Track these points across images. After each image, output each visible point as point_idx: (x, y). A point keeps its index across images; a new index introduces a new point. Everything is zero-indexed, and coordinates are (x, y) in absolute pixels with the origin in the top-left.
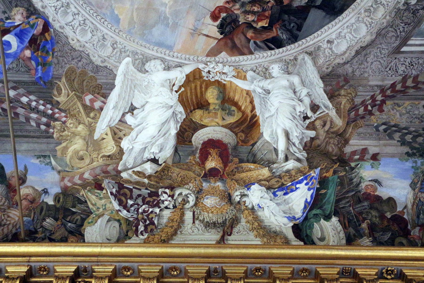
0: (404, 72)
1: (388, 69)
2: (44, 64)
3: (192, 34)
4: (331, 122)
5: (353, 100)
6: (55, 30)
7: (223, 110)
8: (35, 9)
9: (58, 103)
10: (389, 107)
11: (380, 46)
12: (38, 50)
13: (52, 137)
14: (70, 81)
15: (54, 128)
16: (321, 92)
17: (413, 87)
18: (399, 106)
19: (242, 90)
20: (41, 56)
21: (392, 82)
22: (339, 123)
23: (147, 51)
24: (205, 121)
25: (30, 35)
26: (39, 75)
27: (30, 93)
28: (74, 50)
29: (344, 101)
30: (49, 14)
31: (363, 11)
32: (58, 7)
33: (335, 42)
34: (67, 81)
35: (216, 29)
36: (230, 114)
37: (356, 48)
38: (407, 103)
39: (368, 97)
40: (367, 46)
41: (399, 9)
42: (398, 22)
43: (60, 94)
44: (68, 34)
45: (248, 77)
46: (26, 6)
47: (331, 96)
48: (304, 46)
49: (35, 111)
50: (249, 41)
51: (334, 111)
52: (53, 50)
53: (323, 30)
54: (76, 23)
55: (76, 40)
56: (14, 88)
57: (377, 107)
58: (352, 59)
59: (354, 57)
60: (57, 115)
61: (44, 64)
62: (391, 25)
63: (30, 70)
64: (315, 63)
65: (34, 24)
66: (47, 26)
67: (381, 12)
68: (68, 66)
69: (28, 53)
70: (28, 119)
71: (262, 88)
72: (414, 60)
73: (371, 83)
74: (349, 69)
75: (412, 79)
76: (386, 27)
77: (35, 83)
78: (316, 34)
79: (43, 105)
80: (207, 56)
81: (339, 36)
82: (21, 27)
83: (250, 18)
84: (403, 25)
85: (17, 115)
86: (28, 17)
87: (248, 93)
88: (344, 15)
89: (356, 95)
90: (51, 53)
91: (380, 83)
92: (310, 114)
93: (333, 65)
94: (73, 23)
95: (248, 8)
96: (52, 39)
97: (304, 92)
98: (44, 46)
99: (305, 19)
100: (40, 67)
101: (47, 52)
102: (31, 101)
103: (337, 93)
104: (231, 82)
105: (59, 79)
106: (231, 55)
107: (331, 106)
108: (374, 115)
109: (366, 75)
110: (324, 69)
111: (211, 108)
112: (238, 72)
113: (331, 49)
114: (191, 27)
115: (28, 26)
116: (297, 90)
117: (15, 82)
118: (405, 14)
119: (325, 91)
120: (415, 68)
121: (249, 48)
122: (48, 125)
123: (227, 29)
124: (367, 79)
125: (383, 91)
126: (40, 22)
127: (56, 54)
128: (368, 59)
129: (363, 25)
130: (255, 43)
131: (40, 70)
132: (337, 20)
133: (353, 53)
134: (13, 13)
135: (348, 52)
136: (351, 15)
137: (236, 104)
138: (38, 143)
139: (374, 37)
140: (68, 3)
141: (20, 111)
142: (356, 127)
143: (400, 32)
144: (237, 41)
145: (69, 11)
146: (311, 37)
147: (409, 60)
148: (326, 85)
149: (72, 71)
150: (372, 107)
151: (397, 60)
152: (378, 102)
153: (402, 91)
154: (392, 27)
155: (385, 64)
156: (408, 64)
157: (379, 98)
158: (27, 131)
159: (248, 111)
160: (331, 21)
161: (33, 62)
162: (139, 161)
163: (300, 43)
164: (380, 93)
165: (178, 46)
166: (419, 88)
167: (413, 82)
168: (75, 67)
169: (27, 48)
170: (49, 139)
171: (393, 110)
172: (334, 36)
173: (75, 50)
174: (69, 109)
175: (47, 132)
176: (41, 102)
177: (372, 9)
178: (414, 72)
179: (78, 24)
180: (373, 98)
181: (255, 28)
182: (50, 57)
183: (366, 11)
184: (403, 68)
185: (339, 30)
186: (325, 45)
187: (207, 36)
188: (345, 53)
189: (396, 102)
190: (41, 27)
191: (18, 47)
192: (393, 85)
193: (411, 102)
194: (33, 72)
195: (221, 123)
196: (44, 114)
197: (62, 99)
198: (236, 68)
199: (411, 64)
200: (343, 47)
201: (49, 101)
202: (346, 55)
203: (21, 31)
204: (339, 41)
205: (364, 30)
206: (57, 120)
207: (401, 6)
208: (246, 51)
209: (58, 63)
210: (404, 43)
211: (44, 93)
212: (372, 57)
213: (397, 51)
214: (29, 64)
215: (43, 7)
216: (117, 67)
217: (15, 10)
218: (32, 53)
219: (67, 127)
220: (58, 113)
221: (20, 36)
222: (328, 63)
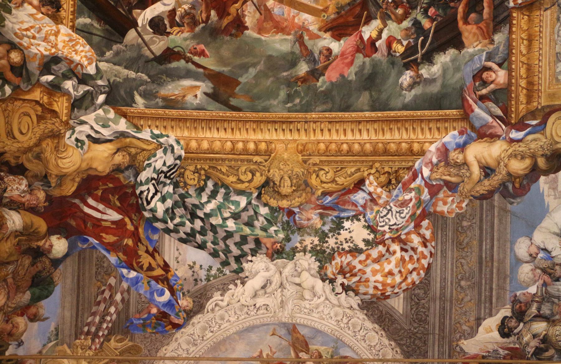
2: (144, 326)
6: (174, 334)
8: (191, 317)
9: (109, 340)
12: (156, 320)
13: (76, 338)
15: (85, 339)
20: (151, 322)
25: (170, 313)
26: (135, 322)
27: (118, 313)
30: (187, 329)
32: (193, 337)
34: (128, 347)
43: (117, 341)
44: (171, 345)
46: (194, 309)
49: (102, 320)
52: (157, 333)
55: (165, 352)
56: (123, 300)
60: (97, 340)
61: (144, 326)
63: (140, 313)
65: (179, 316)
66: (178, 327)
68: (143, 347)
69: (154, 311)
70: (94, 314)
77: (127, 319)
79: (107, 327)
82: (176, 305)
85: (99, 304)
86: (185, 311)
90: (154, 331)
94: (180, 349)
96: (166, 331)
98: (160, 325)
100: (142, 322)
101: (155, 328)
102: (111, 315)
105: (131, 340)
115: (177, 310)
117: (128, 301)
126: (180, 321)
127: (153, 335)
131: (138, 322)
134: (188, 298)
138: (71, 326)
140: (196, 345)
145: (191, 345)
158: (83, 314)
161: (146, 316)
168: (142, 353)
169: (159, 310)
170: (74, 336)
173: (157, 352)
174: (103, 351)
175: (81, 333)
176: (110, 325)
179: (180, 353)
182: (151, 331)
190: (177, 322)
191: (159, 302)
194: (138, 316)
196: (99, 328)
197: (113, 343)
201: (111, 332)
203: (173, 305)
206: (93, 340)
209: (145, 338)
211: (119, 326)
214: (144, 312)
215: (193, 323)
217: (190, 300)
218: (154, 315)
219: (86, 351)
220: (99, 341)
221: (169, 304)
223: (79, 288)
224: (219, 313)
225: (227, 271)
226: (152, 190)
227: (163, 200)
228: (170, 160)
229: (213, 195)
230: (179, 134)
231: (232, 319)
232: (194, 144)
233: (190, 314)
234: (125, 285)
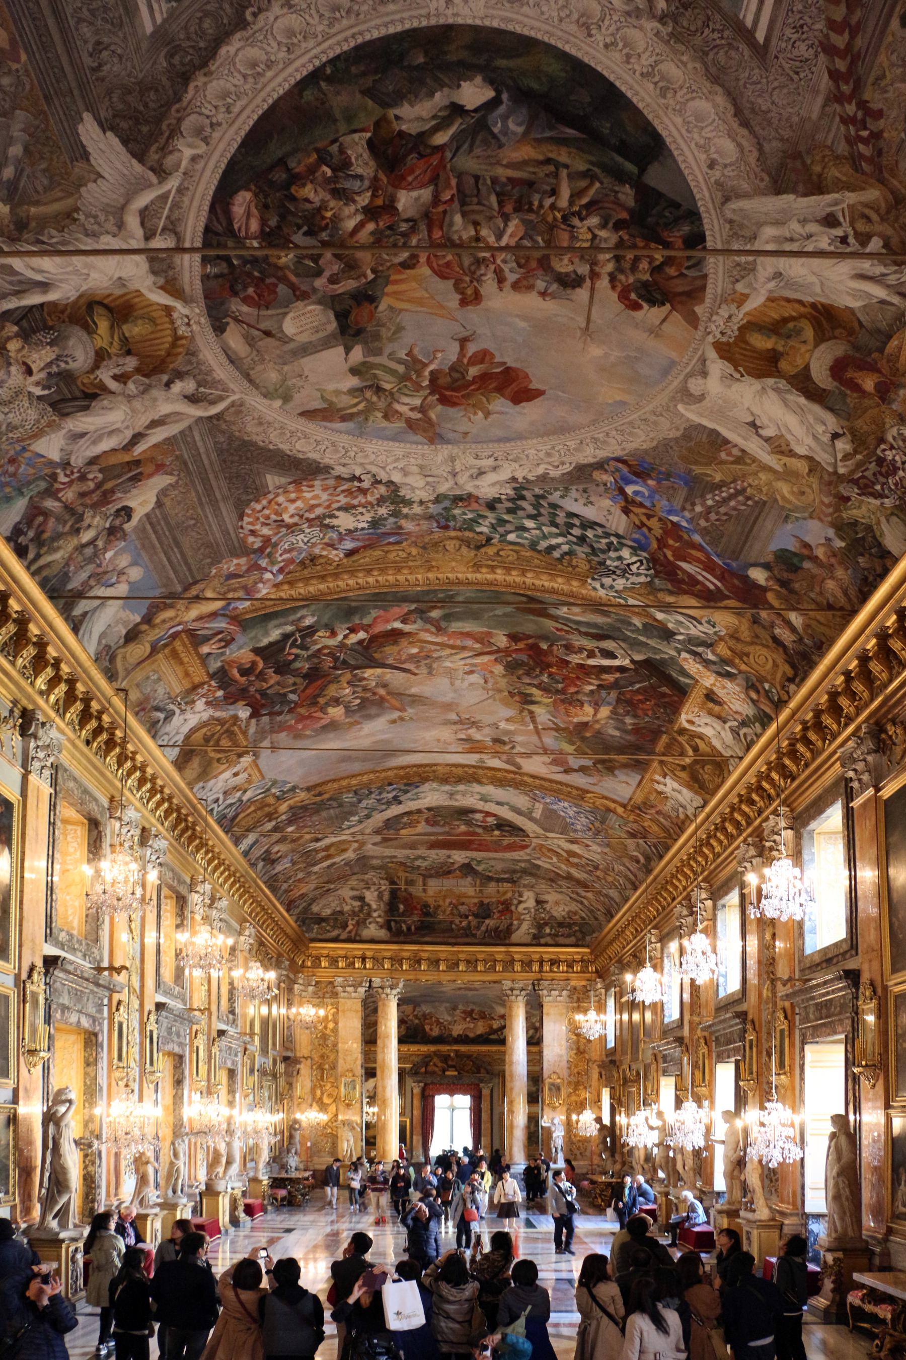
0: (812, 46)
1: (795, 77)
3: (657, 336)
4: (867, 205)
5: (837, 157)
7: (789, 337)
10: (877, 96)
11: (741, 83)
14: (696, 463)
16: (804, 202)
17: (852, 37)
18: (884, 76)
19: (764, 305)
21: (826, 75)
22: (872, 194)
23: (672, 387)
24: (800, 362)
28: (655, 448)
29: (834, 172)
31: (663, 101)
33: (715, 156)
35: (655, 310)
36: (799, 332)
37: (735, 125)
38: (882, 58)
39: (842, 128)
40: (735, 105)
41: (671, 35)
42: (698, 40)
45: (746, 291)
47: (817, 187)
48: (710, 206)
50: (682, 275)
51: (847, 194)
53: (686, 172)
54: (619, 438)
56: (693, 504)
57: (868, 120)
58: (756, 136)
59: (752, 132)
61: (668, 476)
62: (702, 54)
64: (746, 196)
67: (671, 69)
71: (769, 280)
72: (791, 20)
73: (815, 116)
74: (773, 146)
75: (832, 35)
76: (705, 64)
78: (692, 184)
80: (696, 328)
81: (704, 148)
83: (644, 265)
84: (706, 31)
87: (771, 299)
88: (664, 134)
89: (830, 148)
91: (820, 100)
92: (839, 232)
93: (757, 170)
95: (627, 265)
97: (795, 226)
99: (660, 195)
103: (815, 178)
104: (745, 314)
105: (690, 471)
106: (702, 301)
107: (836, 196)
108: (882, 131)
109: (795, 119)
110: (762, 185)
111: (781, 349)
112: (733, 300)
113: (726, 166)
114: (646, 335)
116: (788, 235)
117: (686, 500)
118: (685, 24)
119: (805, 195)
120: (809, 21)
121: (695, 278)
122: (748, 498)
123: (658, 297)
124: (803, 120)
125: (838, 98)
128: (764, 108)
129: (691, 104)
130: (688, 268)
132: (672, 147)
133: (744, 132)
135: (739, 139)
136: (666, 120)
137: (785, 320)
139: (720, 90)
141: (723, 510)
142: (893, 172)
143: (722, 38)
144: (680, 289)
146: (695, 191)
147: (788, 32)
148: (794, 191)
149: (682, 458)
150: (865, 128)
151: (781, 56)
152: (860, 114)
153: (852, 62)
154: (706, 54)
155: (783, 79)
156: (796, 36)
157: (851, 109)
159: (802, 309)
160: (671, 155)
162: (830, 449)
163: (702, 209)
164: (842, 104)
165: (674, 355)
166: (859, 23)
167: (841, 33)
171: (886, 92)
172: (703, 157)
177: (661, 84)
178: (818, 26)
180: (846, 120)
181: (662, 264)
183: (664, 97)
184: (803, 47)
185: (693, 146)
186: (717, 174)
187: (664, 321)
188: (739, 145)
189: (871, 80)
192: (834, 75)
193: (882, 50)
195: (810, 347)
198: (725, 300)
199: (798, 28)
200: (728, 146)
202: (745, 143)
204: (713, 149)
205: (702, 105)
207: (665, 30)
208: (698, 283)
210: (747, 35)
212: (760, 101)
213: (761, 52)
216: (688, 420)
221: (629, 482)
222: (752, 176)
223: (747, 536)
224: (555, 459)
225: (537, 491)
226: (634, 568)
227: (620, 558)
228: (607, 581)
229: (551, 548)
230: (593, 594)
231: (533, 451)
232: (575, 583)
233: (600, 465)
234: (687, 514)
